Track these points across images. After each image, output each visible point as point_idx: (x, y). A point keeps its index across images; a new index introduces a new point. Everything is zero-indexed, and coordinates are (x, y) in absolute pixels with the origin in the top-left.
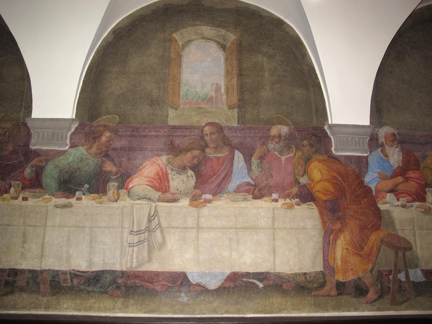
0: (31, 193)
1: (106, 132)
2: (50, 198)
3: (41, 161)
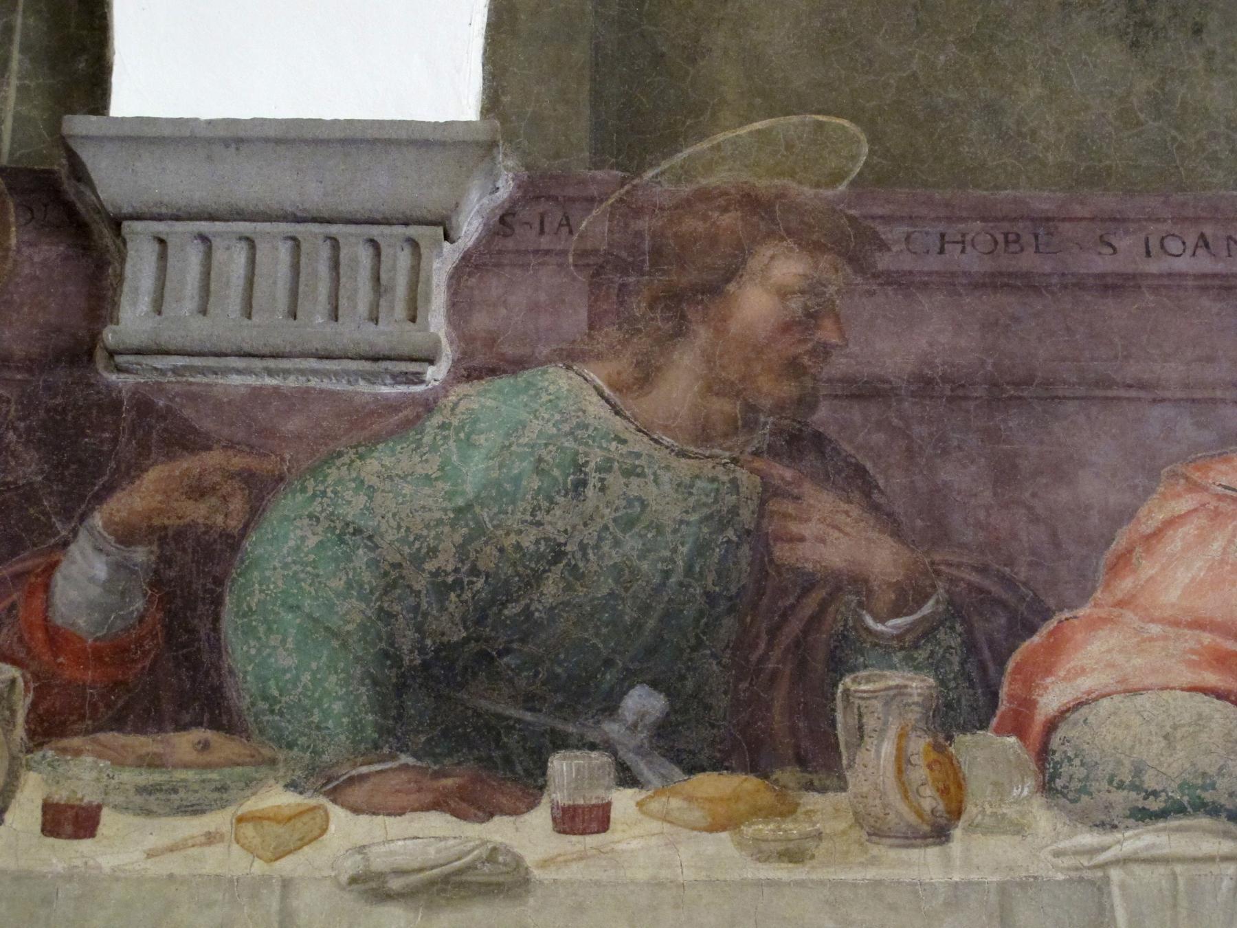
0: (119, 763)
1: (765, 252)
2: (313, 809)
3: (198, 491)
